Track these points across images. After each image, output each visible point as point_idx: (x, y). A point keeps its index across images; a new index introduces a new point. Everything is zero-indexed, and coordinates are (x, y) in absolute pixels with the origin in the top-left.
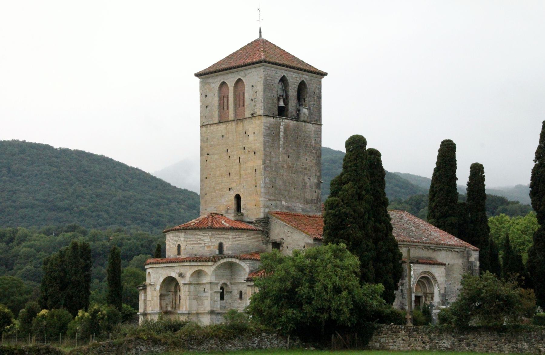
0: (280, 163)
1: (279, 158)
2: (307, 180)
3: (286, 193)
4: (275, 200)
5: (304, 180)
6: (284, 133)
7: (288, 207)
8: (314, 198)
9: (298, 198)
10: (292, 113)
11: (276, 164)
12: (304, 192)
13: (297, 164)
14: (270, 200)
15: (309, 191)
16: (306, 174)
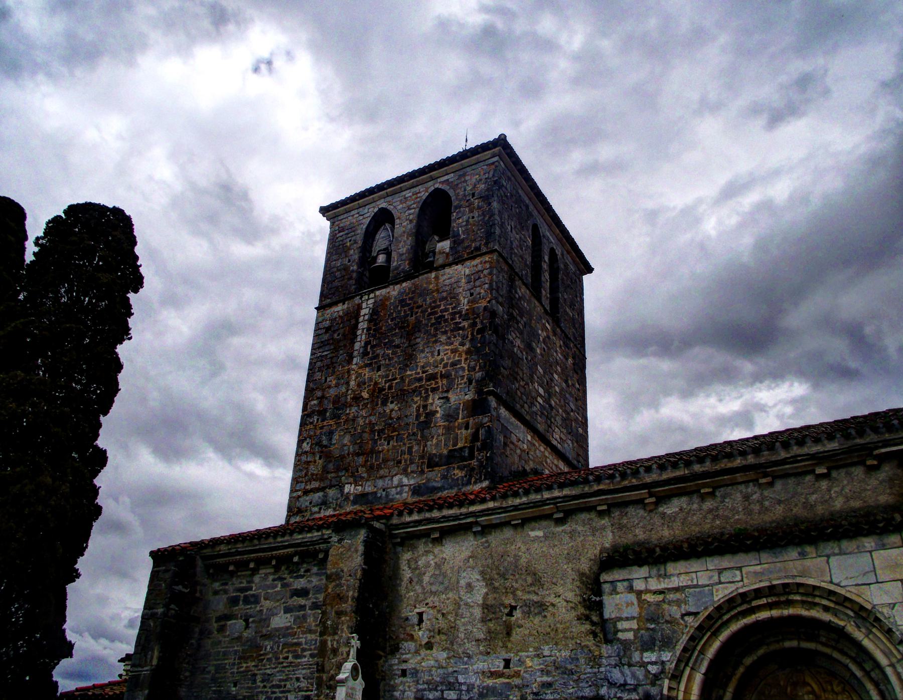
0: (350, 392)
1: (348, 383)
2: (435, 402)
3: (361, 460)
4: (322, 489)
5: (425, 407)
6: (370, 321)
7: (361, 498)
8: (460, 445)
9: (400, 462)
10: (397, 268)
11: (336, 400)
12: (425, 439)
13: (402, 378)
14: (306, 492)
15: (440, 431)
16: (434, 390)
